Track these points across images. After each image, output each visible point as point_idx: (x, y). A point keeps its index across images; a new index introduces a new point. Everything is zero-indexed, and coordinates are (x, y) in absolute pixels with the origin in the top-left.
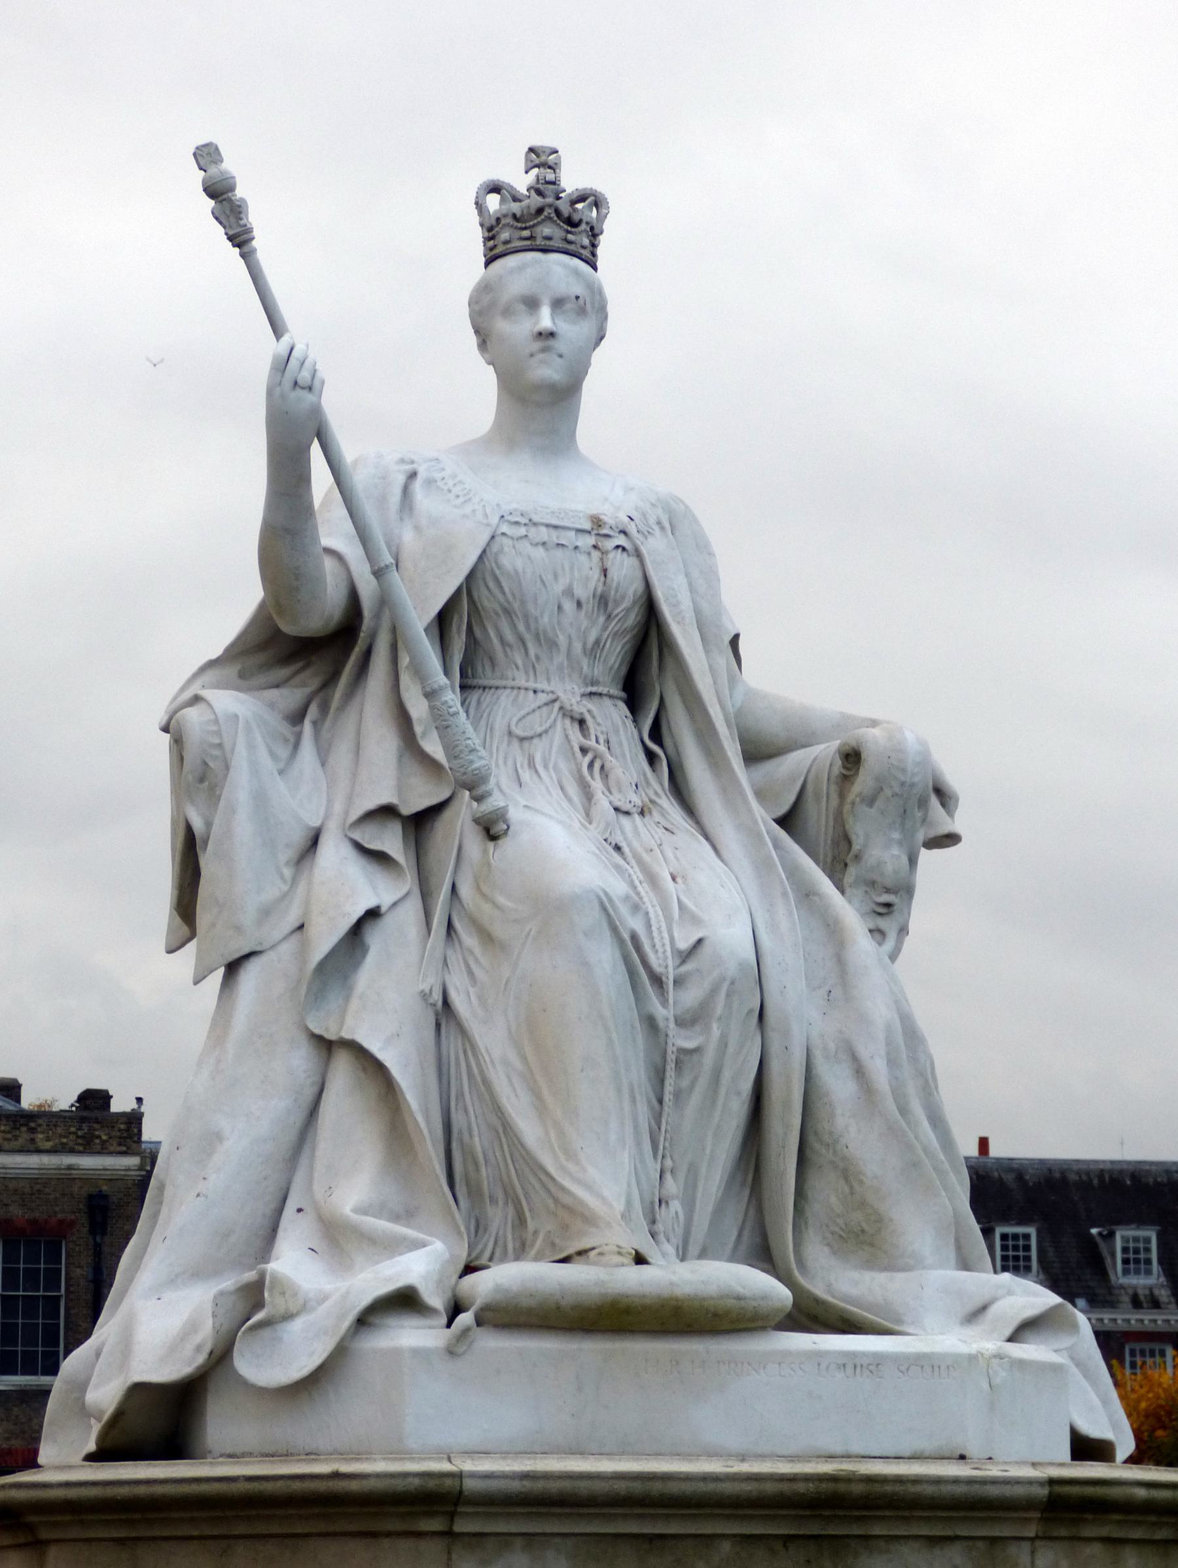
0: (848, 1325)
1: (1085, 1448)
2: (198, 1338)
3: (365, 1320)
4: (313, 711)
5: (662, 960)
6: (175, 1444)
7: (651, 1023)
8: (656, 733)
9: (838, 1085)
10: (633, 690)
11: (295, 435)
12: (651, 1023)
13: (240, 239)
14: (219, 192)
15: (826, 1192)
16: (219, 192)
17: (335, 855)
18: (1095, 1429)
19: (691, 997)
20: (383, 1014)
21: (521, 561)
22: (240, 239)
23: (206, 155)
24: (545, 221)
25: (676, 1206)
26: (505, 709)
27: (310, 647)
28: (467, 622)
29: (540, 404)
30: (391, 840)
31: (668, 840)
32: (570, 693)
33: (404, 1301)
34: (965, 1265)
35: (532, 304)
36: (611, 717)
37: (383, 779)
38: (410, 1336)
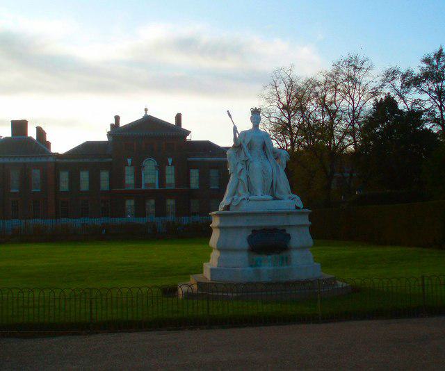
1: (297, 208)
9: (279, 182)
14: (229, 114)
16: (229, 114)
17: (240, 164)
18: (299, 206)
31: (267, 163)
33: (244, 199)
37: (243, 157)
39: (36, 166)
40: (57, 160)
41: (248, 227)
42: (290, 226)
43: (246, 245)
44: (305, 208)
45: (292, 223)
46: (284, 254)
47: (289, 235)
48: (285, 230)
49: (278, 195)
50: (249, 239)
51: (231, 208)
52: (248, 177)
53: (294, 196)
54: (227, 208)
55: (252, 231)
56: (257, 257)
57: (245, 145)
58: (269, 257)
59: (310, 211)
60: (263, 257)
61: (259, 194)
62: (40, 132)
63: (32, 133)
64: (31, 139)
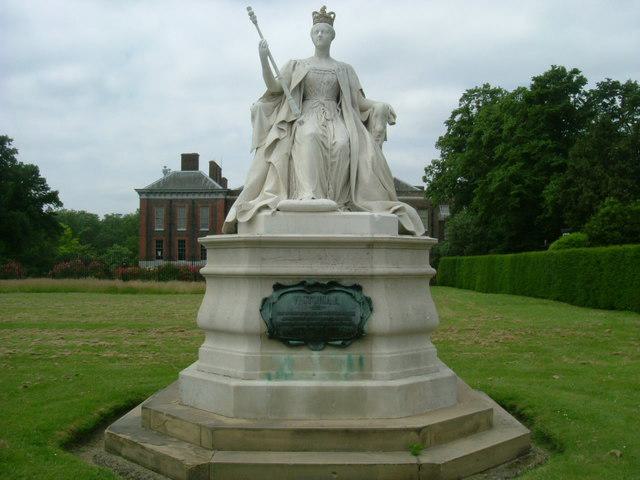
0: (359, 210)
1: (403, 231)
3: (260, 210)
6: (236, 232)
7: (325, 158)
8: (340, 105)
9: (362, 166)
11: (265, 54)
12: (325, 158)
13: (255, 23)
14: (251, 15)
15: (360, 189)
16: (251, 15)
18: (410, 227)
22: (255, 23)
23: (249, 9)
24: (325, 18)
25: (331, 190)
26: (309, 104)
27: (275, 95)
29: (323, 50)
32: (322, 99)
33: (266, 207)
34: (391, 200)
37: (282, 115)
38: (266, 213)
39: (205, 203)
40: (228, 197)
42: (372, 277)
43: (257, 323)
44: (426, 234)
45: (380, 268)
46: (355, 351)
47: (369, 301)
48: (358, 288)
49: (359, 203)
53: (399, 205)
55: (277, 287)
56: (281, 354)
58: (316, 355)
61: (306, 196)
62: (215, 169)
63: (204, 168)
64: (201, 177)
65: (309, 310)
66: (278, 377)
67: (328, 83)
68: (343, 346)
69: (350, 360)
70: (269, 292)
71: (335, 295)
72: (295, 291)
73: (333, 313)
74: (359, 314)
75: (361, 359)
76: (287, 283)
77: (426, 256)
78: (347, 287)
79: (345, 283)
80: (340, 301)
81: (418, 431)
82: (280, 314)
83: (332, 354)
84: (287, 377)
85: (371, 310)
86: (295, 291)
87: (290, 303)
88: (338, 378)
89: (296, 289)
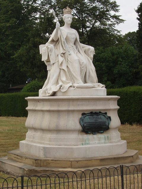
2: (57, 89)
4: (55, 46)
5: (81, 63)
9: (91, 71)
10: (75, 44)
12: (81, 67)
19: (83, 66)
20: (64, 67)
21: (69, 36)
28: (67, 39)
30: (63, 55)
31: (79, 55)
33: (71, 86)
35: (68, 18)
36: (74, 46)
37: (62, 51)
38: (72, 88)
41: (78, 111)
42: (110, 110)
43: (79, 127)
47: (110, 118)
48: (106, 113)
50: (81, 120)
51: (58, 94)
52: (67, 67)
54: (54, 94)
55: (83, 114)
56: (85, 136)
57: (63, 40)
58: (95, 136)
59: (119, 97)
60: (90, 136)
65: (94, 121)
66: (85, 144)
67: (74, 38)
68: (101, 133)
69: (105, 137)
70: (80, 116)
71: (100, 116)
72: (89, 115)
73: (101, 122)
74: (107, 122)
75: (108, 137)
76: (86, 113)
77: (116, 102)
78: (103, 113)
79: (102, 112)
80: (102, 119)
81: (132, 156)
82: (85, 123)
83: (100, 136)
84: (88, 144)
85: (111, 120)
86: (89, 115)
87: (88, 119)
88: (102, 143)
89: (89, 114)
